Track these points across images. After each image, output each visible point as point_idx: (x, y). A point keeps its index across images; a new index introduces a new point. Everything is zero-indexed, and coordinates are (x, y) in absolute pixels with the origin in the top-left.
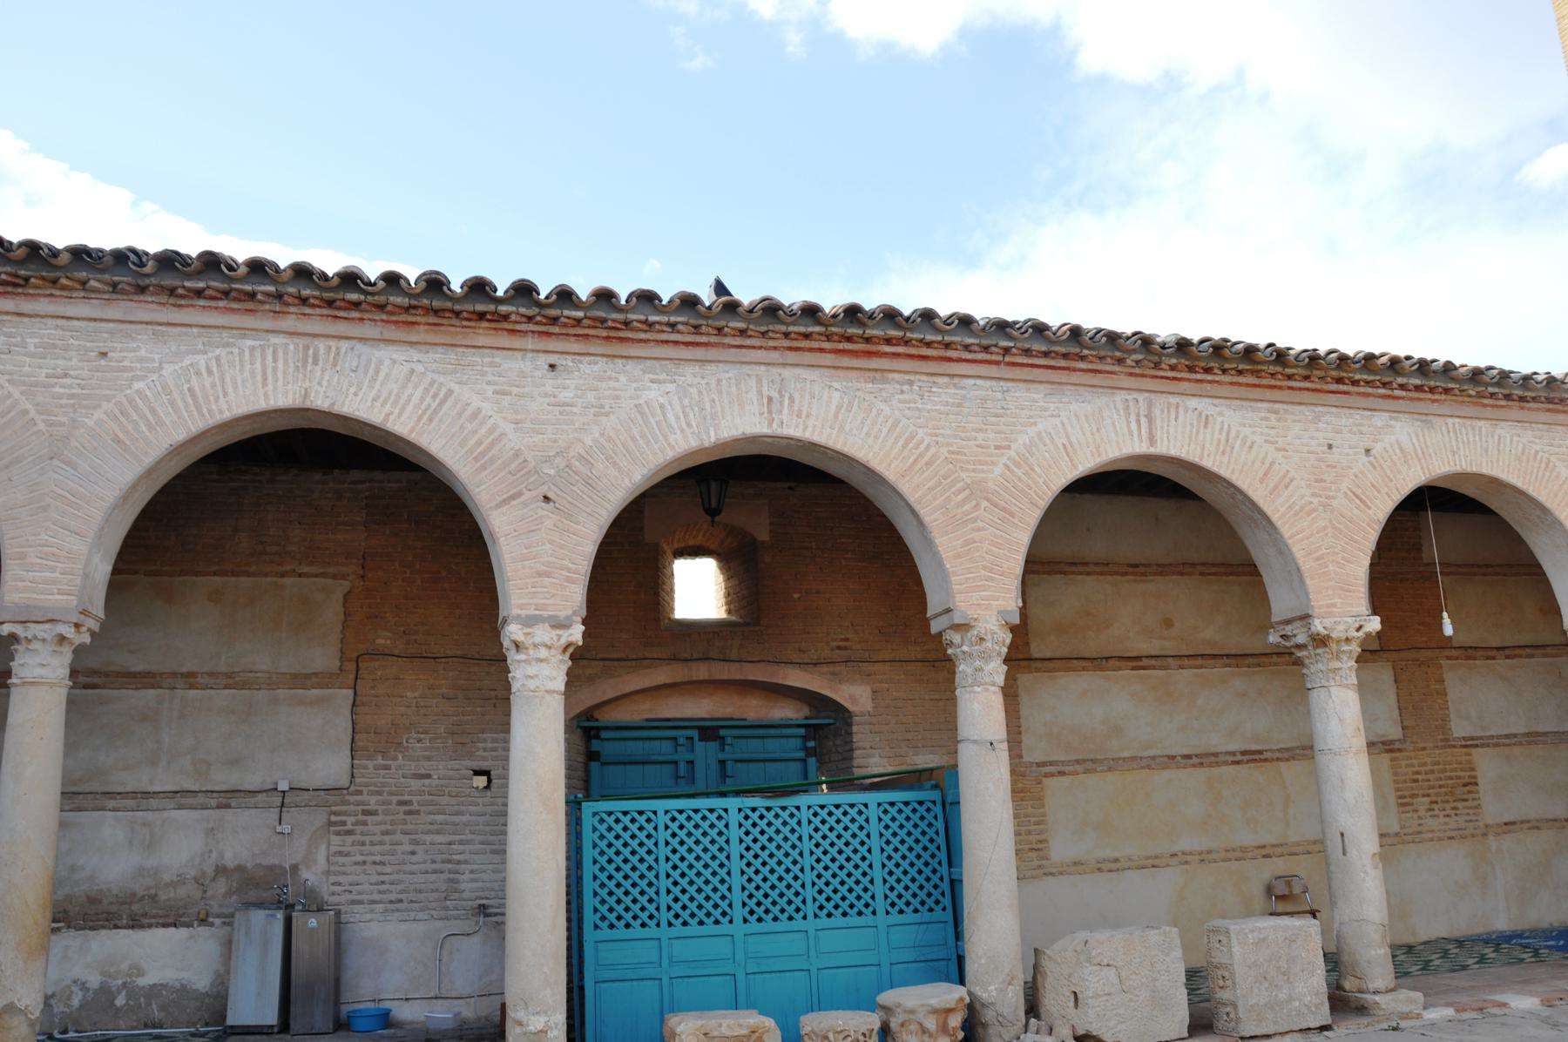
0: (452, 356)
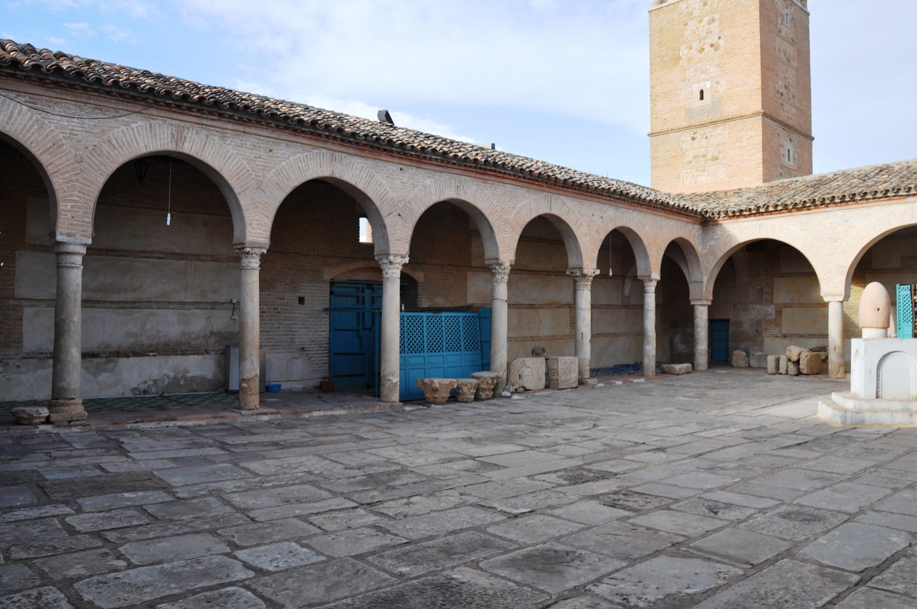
0: (374, 162)
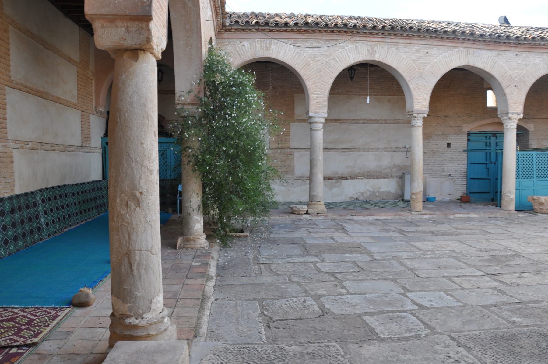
0: (497, 52)
